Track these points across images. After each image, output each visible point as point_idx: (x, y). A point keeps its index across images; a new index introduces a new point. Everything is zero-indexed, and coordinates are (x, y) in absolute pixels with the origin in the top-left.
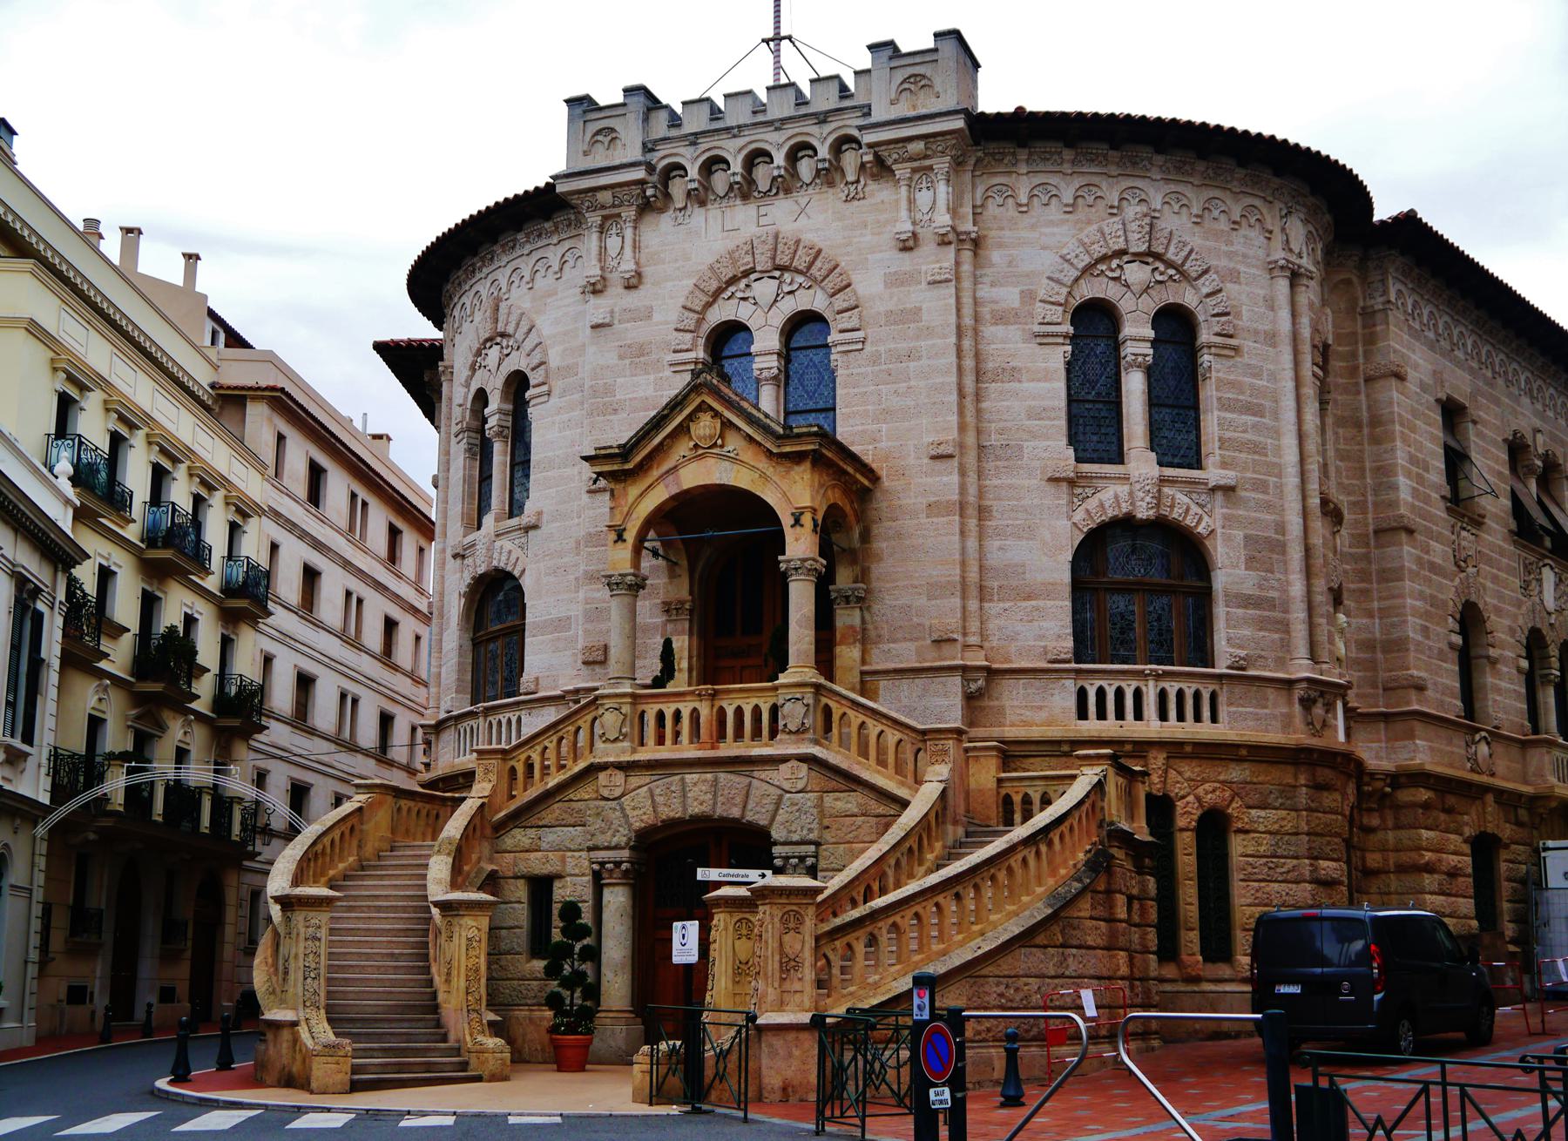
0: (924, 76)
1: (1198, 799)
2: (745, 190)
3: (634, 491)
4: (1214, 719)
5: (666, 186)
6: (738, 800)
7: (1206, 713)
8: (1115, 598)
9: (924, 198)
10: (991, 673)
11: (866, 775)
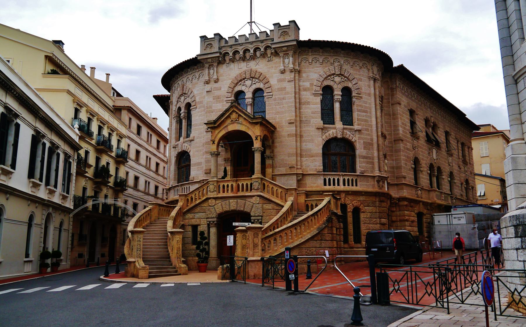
1: (353, 205)
2: (244, 59)
3: (217, 132)
4: (356, 185)
5: (224, 58)
6: (243, 206)
7: (354, 184)
9: (287, 61)
10: (303, 175)
11: (273, 200)
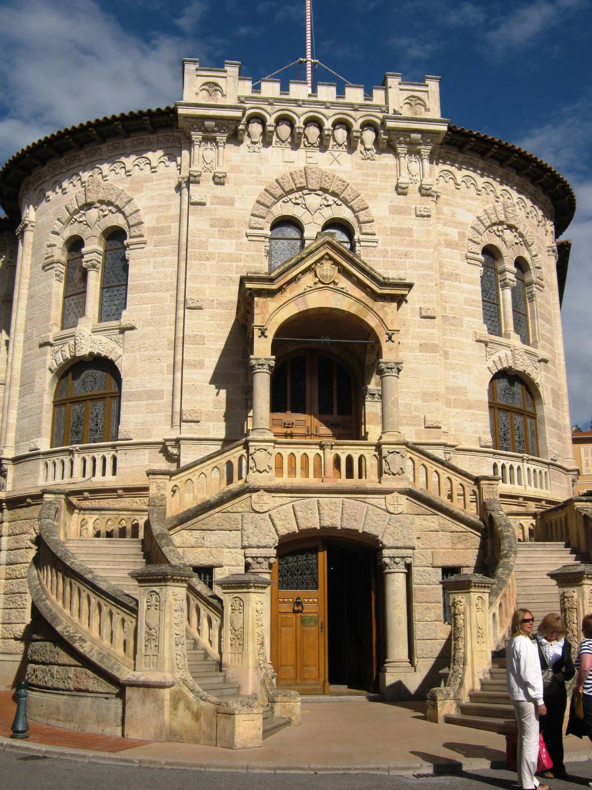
0: (419, 99)
3: (272, 304)
8: (501, 414)
